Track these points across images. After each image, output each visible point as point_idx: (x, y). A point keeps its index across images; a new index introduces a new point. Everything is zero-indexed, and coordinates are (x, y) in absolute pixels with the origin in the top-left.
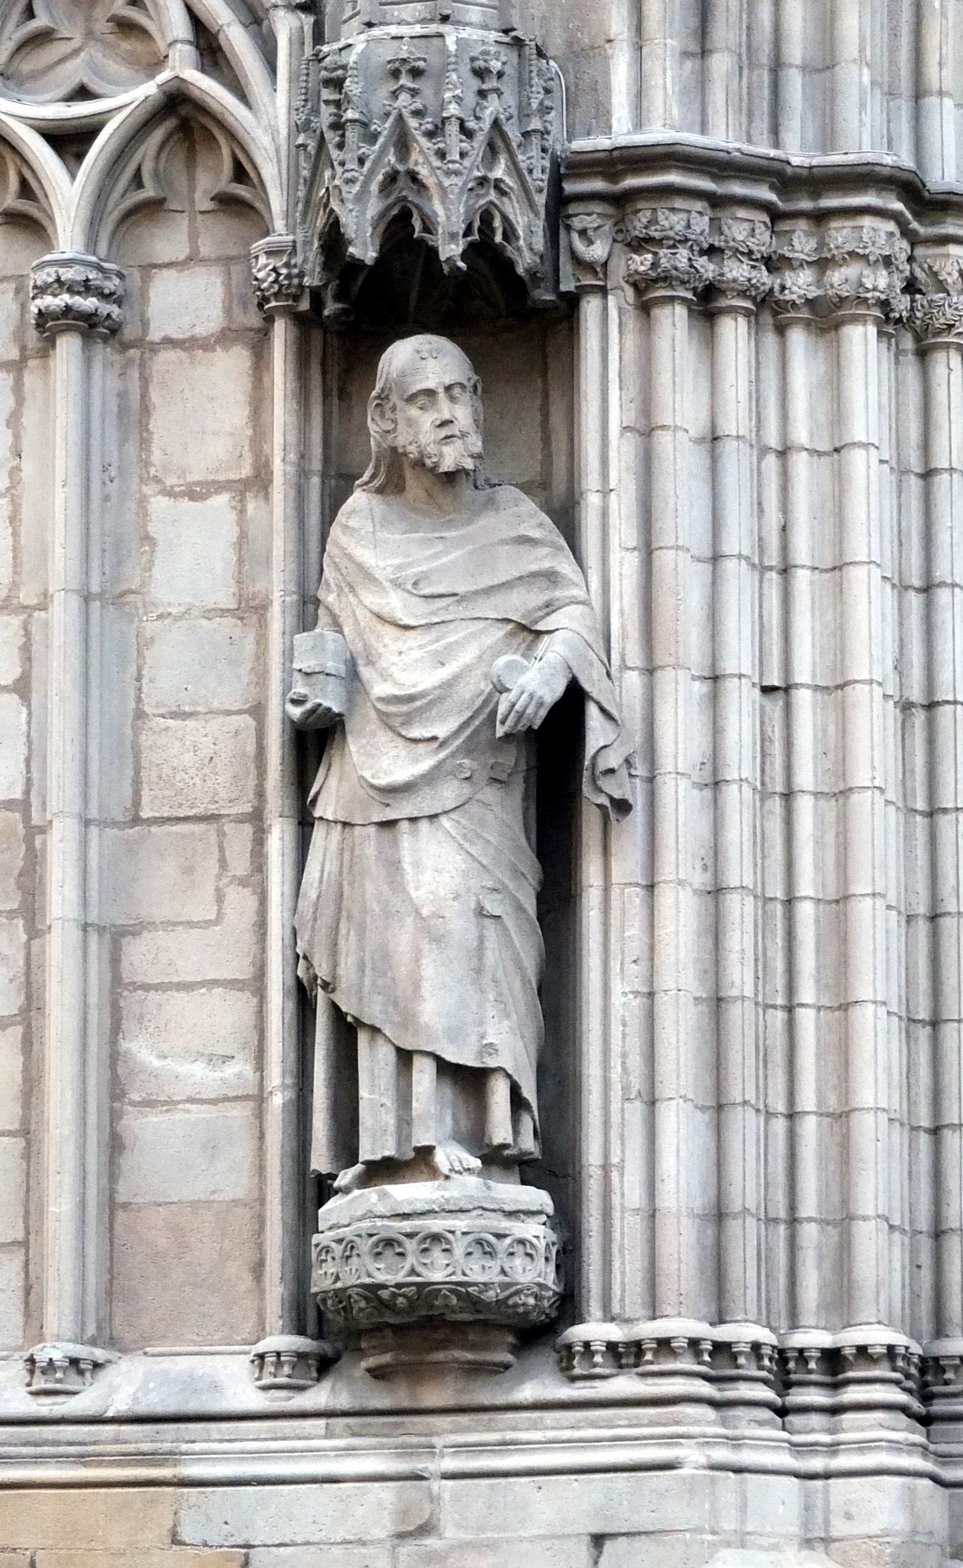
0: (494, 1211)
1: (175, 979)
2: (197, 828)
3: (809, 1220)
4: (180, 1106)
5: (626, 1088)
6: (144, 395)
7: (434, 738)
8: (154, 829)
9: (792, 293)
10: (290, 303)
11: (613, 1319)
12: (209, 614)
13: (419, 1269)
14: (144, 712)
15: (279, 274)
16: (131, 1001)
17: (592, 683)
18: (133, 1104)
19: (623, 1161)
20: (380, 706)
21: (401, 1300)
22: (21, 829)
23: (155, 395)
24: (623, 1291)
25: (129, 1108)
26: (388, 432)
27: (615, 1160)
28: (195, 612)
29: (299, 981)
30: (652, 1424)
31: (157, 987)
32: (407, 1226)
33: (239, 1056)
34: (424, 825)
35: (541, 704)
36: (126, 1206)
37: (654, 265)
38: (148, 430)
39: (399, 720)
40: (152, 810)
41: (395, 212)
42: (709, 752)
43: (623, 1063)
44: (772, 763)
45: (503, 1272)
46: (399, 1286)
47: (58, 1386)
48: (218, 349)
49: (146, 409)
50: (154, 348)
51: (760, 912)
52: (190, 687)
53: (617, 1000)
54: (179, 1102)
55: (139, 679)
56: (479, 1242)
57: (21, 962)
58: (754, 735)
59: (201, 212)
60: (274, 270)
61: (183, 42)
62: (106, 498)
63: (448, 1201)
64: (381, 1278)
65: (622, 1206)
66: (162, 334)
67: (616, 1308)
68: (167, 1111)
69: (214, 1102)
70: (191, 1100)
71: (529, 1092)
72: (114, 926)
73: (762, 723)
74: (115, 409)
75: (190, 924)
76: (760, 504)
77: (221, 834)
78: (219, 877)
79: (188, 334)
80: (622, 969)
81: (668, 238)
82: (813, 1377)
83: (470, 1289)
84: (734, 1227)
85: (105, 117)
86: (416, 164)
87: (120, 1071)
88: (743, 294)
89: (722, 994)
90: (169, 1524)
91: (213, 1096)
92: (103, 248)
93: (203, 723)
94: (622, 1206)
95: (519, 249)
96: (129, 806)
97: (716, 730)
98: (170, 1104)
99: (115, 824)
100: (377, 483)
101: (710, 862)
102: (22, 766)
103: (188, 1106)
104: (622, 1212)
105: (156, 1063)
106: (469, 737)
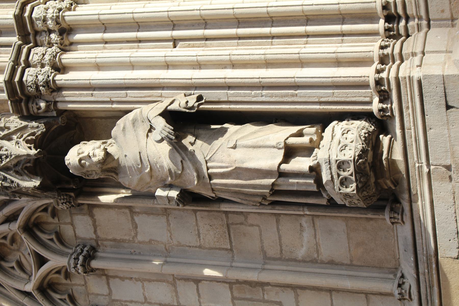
1: (278, 241)
2: (232, 231)
4: (317, 241)
6: (111, 240)
7: (182, 162)
8: (233, 244)
10: (72, 199)
12: (169, 225)
14: (199, 246)
15: (63, 203)
17: (160, 107)
18: (318, 256)
20: (174, 179)
21: (362, 180)
22: (238, 285)
23: (110, 237)
25: (319, 258)
26: (96, 173)
29: (269, 204)
36: (351, 261)
37: (44, 86)
38: (120, 240)
40: (227, 245)
41: (26, 172)
45: (352, 142)
47: (408, 292)
48: (95, 218)
49: (114, 240)
50: (98, 237)
52: (190, 231)
54: (316, 242)
55: (190, 247)
57: (278, 288)
59: (59, 221)
60: (62, 204)
61: (9, 226)
66: (93, 234)
67: (367, 99)
68: (319, 246)
70: (315, 237)
72: (264, 259)
77: (232, 224)
78: (246, 225)
79: (92, 226)
82: (395, 25)
83: (357, 154)
85: (32, 250)
86: (12, 165)
90: (451, 261)
92: (70, 251)
96: (227, 252)
98: (317, 244)
99: (233, 257)
100: (115, 176)
102: (219, 283)
103: (317, 239)
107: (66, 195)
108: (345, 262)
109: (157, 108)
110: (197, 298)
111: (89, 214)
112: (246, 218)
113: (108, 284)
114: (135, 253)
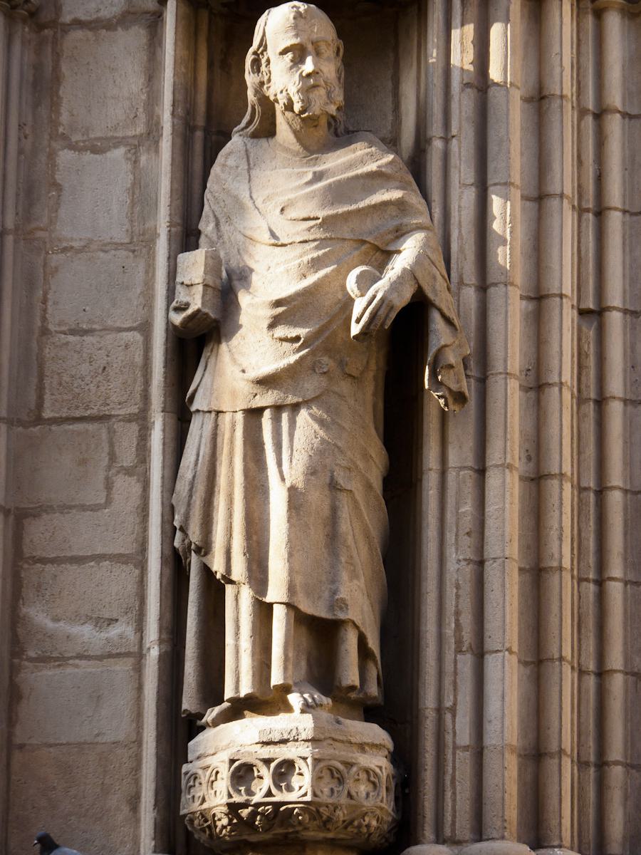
0: (342, 742)
1: (69, 554)
3: (616, 763)
4: (71, 662)
5: (459, 642)
6: (56, 67)
8: (54, 428)
11: (444, 842)
14: (47, 329)
18: (31, 660)
19: (455, 704)
23: (64, 68)
24: (454, 816)
27: (448, 704)
28: (93, 247)
29: (175, 550)
33: (122, 619)
35: (392, 308)
36: (21, 747)
38: (59, 97)
40: (52, 411)
43: (457, 621)
44: (588, 375)
45: (350, 795)
46: (258, 805)
48: (119, 29)
49: (57, 79)
50: (66, 28)
51: (576, 499)
52: (87, 308)
53: (451, 566)
54: (71, 658)
55: (45, 301)
56: (331, 770)
58: (572, 349)
62: (20, 152)
65: (454, 742)
67: (448, 832)
68: (59, 666)
69: (100, 658)
71: (373, 644)
74: (31, 79)
76: (579, 156)
77: (111, 432)
78: (109, 467)
79: (94, 17)
87: (20, 631)
89: (543, 565)
91: (99, 653)
93: (98, 339)
94: (454, 742)
98: (62, 660)
99: (21, 423)
100: (251, 129)
101: (533, 455)
103: (77, 661)
105: (50, 625)
108: (18, 730)
109: (434, 278)
111: (128, 12)
112: (129, 472)
114: (22, 135)
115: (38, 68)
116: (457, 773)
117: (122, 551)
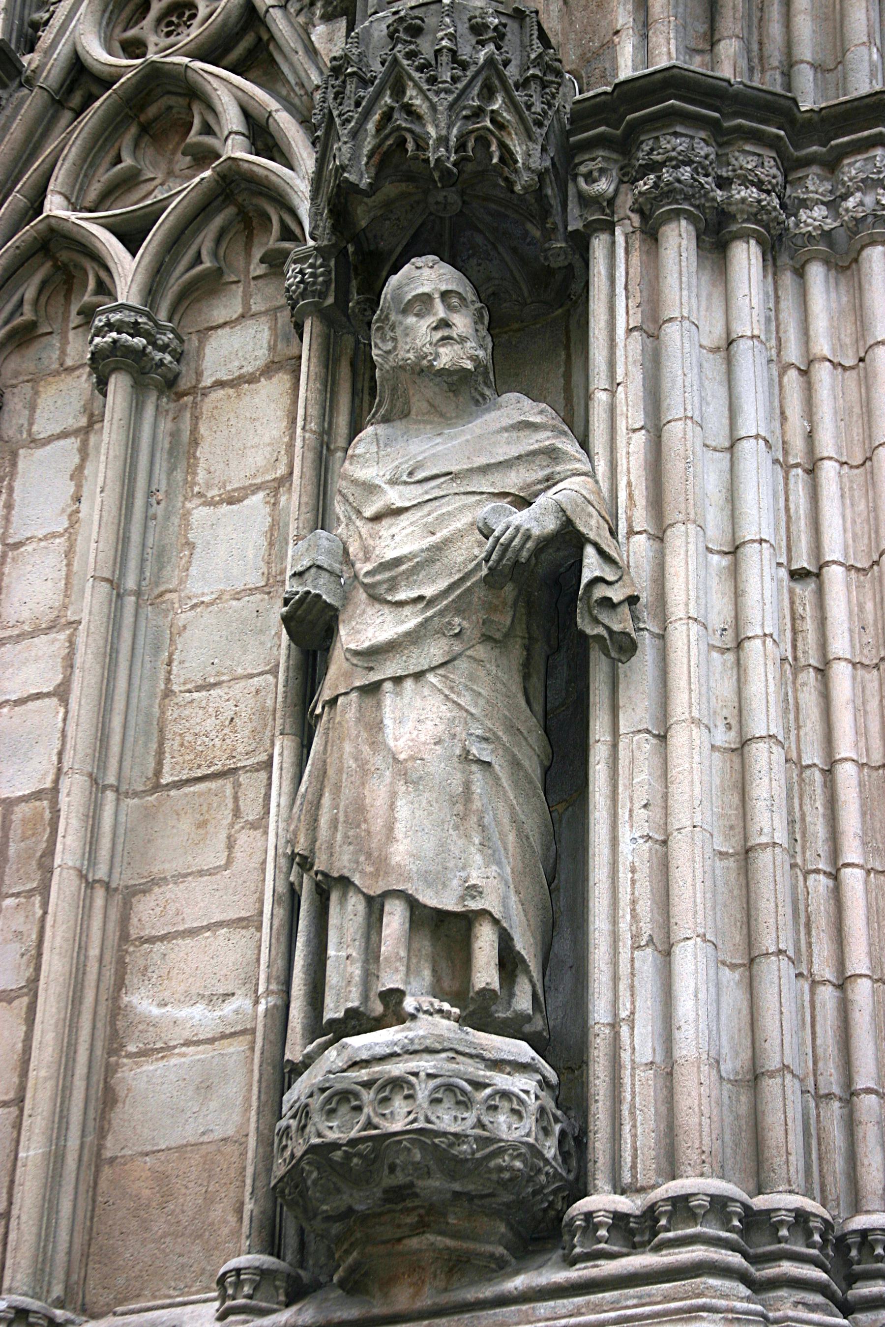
0: (471, 1056)
1: (181, 928)
2: (213, 785)
3: (868, 1091)
4: (177, 1051)
6: (194, 430)
7: (421, 598)
8: (173, 793)
9: (807, 225)
10: (316, 299)
13: (376, 1120)
14: (172, 691)
15: (304, 275)
16: (136, 956)
18: (129, 1055)
19: (633, 1013)
20: (367, 580)
21: (355, 1160)
22: (47, 815)
23: (203, 429)
24: (635, 1157)
25: (125, 1060)
26: (389, 352)
27: (624, 1014)
29: (292, 884)
30: (667, 1299)
31: (162, 938)
32: (364, 1074)
34: (409, 684)
35: (528, 537)
36: (112, 1160)
37: (656, 185)
38: (195, 457)
39: (385, 586)
41: (390, 142)
42: (730, 619)
43: (633, 910)
46: (353, 1142)
48: (262, 379)
49: (195, 442)
52: (216, 661)
53: (625, 847)
54: (175, 1047)
55: (169, 664)
56: (450, 1088)
57: (34, 937)
59: (254, 278)
60: (301, 272)
61: (237, 133)
63: (412, 1041)
64: (332, 1136)
66: (214, 379)
67: (627, 1178)
68: (163, 1057)
69: (211, 1041)
70: (187, 1043)
72: (127, 887)
73: (792, 603)
74: (167, 446)
75: (201, 873)
77: (237, 785)
79: (237, 374)
80: (631, 816)
81: (671, 159)
84: (771, 1086)
85: (165, 203)
86: (411, 99)
88: (754, 218)
91: (210, 1036)
92: (162, 316)
93: (226, 690)
94: (633, 1061)
95: (516, 171)
96: (150, 775)
97: (738, 594)
101: (734, 722)
102: (55, 758)
103: (184, 1049)
104: (633, 1068)
105: (156, 1011)
106: (459, 597)
107: (327, 283)
108: (109, 1142)
110: (14, 697)
111: (273, 362)
113: (64, 435)
114: (154, 502)
115: (175, 435)
116: (637, 1099)
117: (244, 914)
